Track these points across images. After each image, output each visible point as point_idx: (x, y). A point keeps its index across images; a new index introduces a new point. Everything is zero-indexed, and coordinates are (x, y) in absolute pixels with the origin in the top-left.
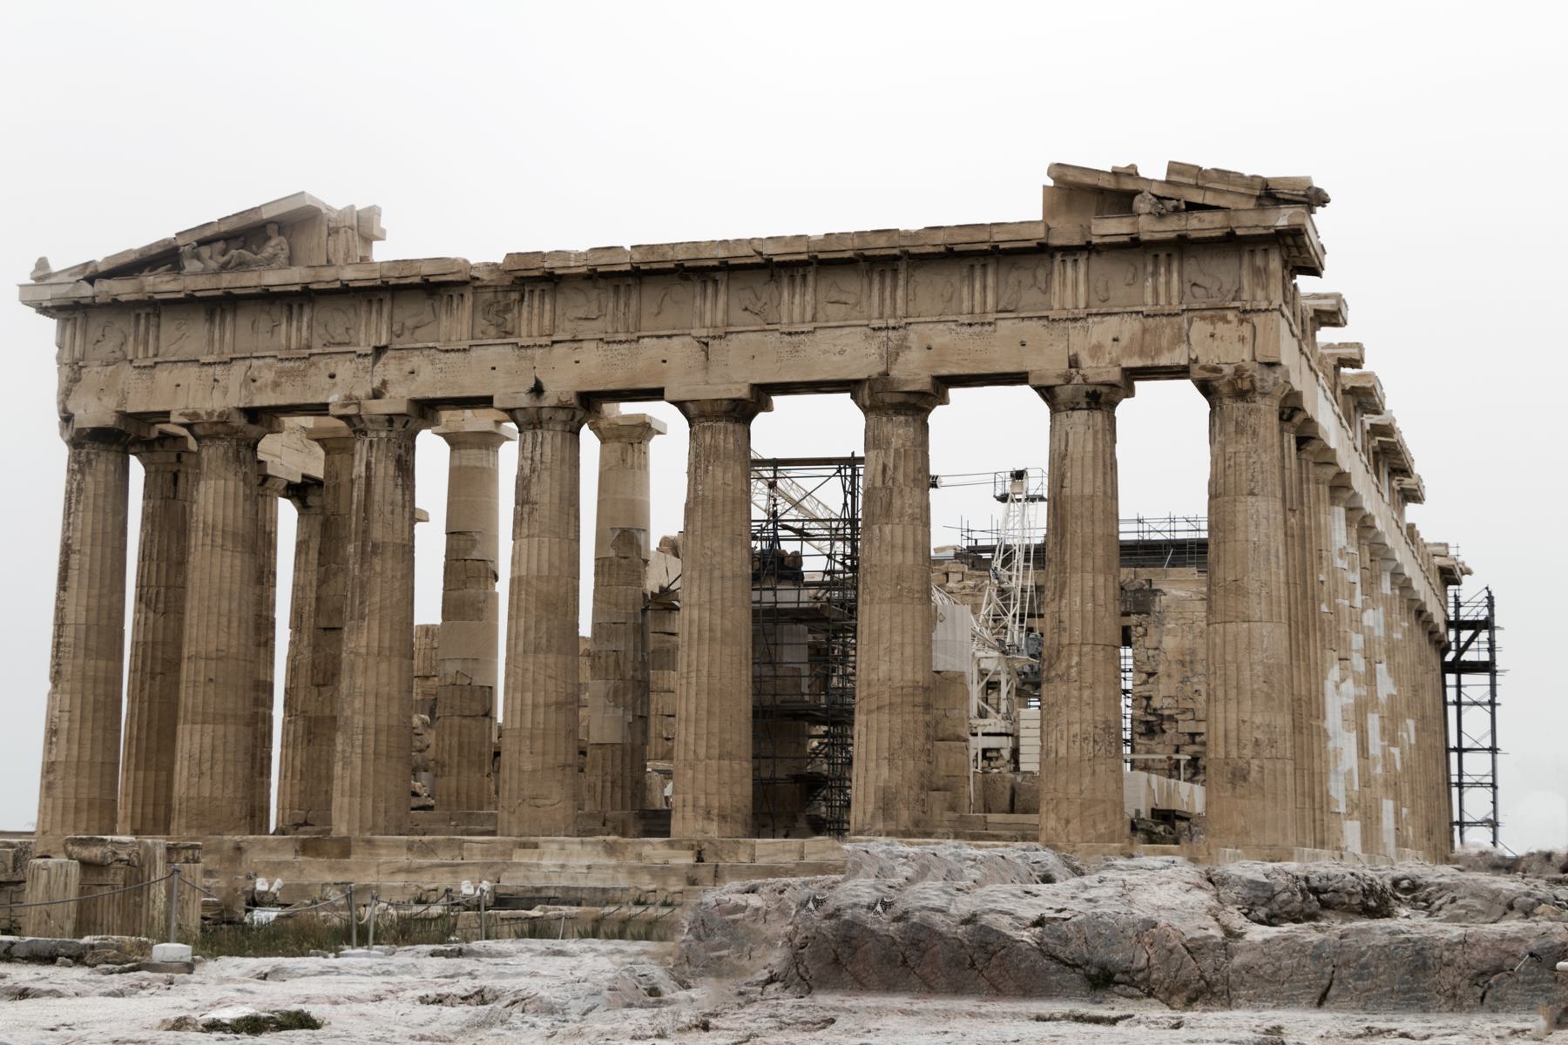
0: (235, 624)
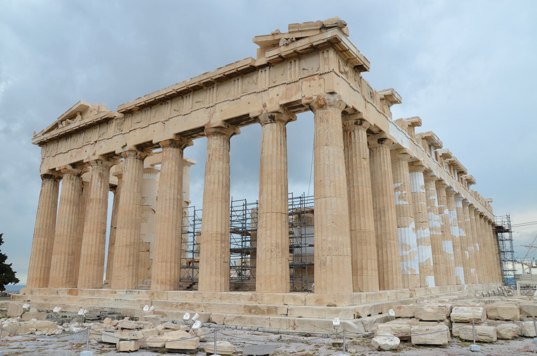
0: (66, 226)
